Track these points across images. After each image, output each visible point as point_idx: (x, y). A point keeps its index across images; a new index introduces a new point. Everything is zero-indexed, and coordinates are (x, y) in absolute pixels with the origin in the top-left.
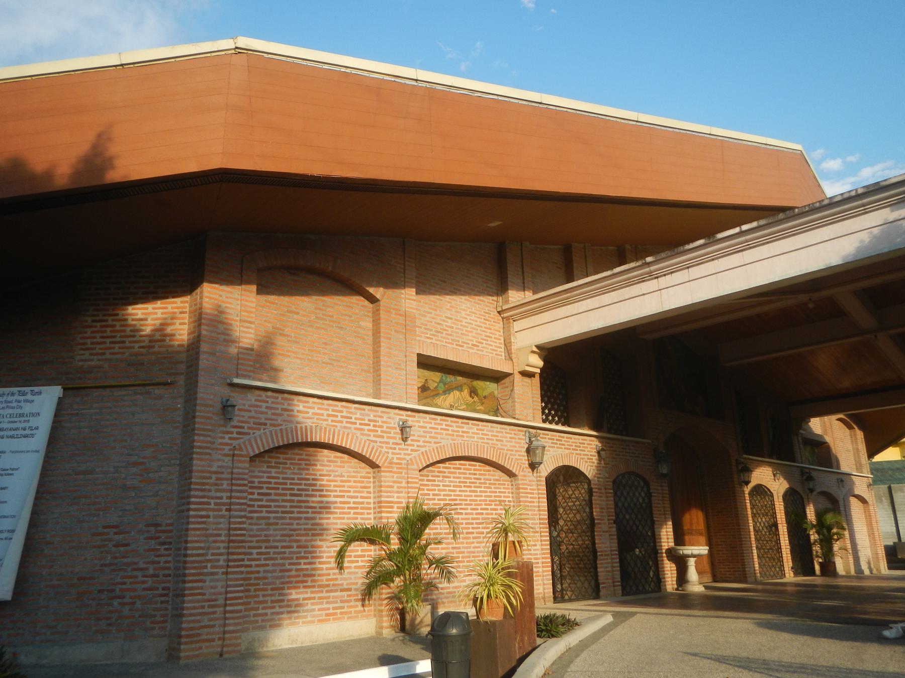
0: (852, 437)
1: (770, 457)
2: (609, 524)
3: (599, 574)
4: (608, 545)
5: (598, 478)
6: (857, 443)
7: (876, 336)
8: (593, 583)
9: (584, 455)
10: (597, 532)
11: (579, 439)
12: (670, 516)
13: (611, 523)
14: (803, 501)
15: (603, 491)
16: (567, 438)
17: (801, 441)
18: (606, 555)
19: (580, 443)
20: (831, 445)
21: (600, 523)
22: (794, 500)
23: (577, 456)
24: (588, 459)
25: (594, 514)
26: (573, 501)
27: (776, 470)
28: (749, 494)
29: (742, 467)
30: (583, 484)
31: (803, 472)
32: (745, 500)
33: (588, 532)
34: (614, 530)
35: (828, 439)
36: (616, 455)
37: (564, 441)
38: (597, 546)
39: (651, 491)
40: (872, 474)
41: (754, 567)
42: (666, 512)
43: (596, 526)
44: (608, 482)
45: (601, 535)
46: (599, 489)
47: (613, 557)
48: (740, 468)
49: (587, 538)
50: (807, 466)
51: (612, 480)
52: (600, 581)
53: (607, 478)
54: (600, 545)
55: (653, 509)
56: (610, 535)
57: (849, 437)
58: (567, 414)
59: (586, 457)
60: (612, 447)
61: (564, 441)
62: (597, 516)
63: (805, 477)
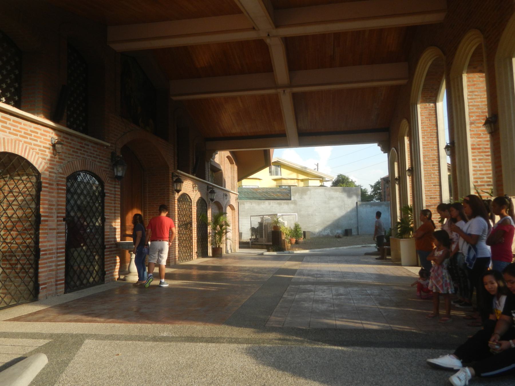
0: (231, 169)
1: (193, 174)
2: (58, 221)
3: (40, 275)
4: (54, 243)
5: (50, 172)
6: (234, 173)
7: (284, 91)
8: (32, 284)
9: (35, 145)
10: (43, 229)
11: (31, 127)
12: (119, 215)
13: (61, 221)
14: (207, 207)
15: (55, 187)
16: (14, 121)
17: (209, 166)
18: (50, 254)
19: (31, 131)
20: (223, 172)
21: (47, 221)
22: (203, 204)
23: (25, 145)
24: (40, 150)
25: (41, 210)
26: (14, 196)
27: (195, 184)
28: (179, 201)
29: (176, 179)
30: (30, 177)
31: (208, 187)
32: (175, 204)
33: (30, 230)
34: (63, 227)
35: (222, 168)
36: (73, 151)
37: (10, 124)
38: (40, 244)
39: (105, 191)
40: (239, 192)
41: (175, 254)
42: (116, 211)
43: (42, 223)
44: (60, 177)
45: (47, 233)
46: (50, 184)
47: (59, 255)
48: (174, 180)
49: (28, 236)
50: (211, 183)
51: (66, 176)
52: (40, 283)
53: (61, 173)
54: (44, 244)
55: (105, 207)
56: (58, 233)
57: (230, 169)
58: (20, 97)
59: (38, 148)
60: (70, 143)
61: (10, 124)
62: (43, 212)
63: (209, 191)
